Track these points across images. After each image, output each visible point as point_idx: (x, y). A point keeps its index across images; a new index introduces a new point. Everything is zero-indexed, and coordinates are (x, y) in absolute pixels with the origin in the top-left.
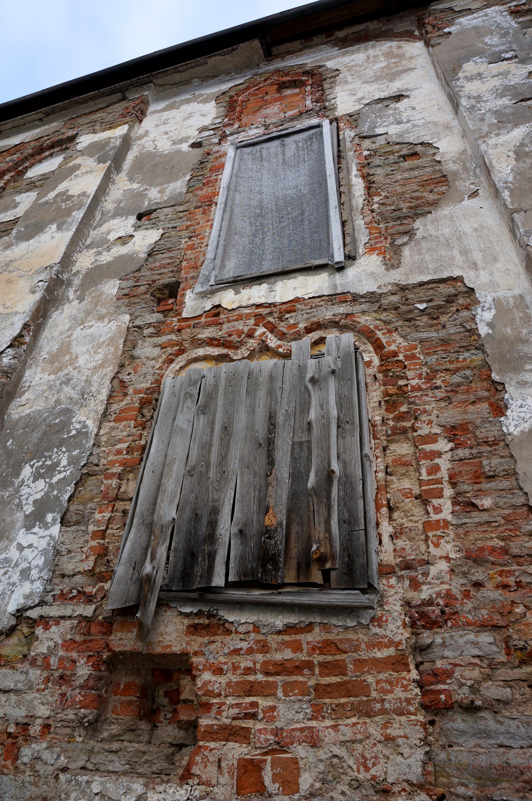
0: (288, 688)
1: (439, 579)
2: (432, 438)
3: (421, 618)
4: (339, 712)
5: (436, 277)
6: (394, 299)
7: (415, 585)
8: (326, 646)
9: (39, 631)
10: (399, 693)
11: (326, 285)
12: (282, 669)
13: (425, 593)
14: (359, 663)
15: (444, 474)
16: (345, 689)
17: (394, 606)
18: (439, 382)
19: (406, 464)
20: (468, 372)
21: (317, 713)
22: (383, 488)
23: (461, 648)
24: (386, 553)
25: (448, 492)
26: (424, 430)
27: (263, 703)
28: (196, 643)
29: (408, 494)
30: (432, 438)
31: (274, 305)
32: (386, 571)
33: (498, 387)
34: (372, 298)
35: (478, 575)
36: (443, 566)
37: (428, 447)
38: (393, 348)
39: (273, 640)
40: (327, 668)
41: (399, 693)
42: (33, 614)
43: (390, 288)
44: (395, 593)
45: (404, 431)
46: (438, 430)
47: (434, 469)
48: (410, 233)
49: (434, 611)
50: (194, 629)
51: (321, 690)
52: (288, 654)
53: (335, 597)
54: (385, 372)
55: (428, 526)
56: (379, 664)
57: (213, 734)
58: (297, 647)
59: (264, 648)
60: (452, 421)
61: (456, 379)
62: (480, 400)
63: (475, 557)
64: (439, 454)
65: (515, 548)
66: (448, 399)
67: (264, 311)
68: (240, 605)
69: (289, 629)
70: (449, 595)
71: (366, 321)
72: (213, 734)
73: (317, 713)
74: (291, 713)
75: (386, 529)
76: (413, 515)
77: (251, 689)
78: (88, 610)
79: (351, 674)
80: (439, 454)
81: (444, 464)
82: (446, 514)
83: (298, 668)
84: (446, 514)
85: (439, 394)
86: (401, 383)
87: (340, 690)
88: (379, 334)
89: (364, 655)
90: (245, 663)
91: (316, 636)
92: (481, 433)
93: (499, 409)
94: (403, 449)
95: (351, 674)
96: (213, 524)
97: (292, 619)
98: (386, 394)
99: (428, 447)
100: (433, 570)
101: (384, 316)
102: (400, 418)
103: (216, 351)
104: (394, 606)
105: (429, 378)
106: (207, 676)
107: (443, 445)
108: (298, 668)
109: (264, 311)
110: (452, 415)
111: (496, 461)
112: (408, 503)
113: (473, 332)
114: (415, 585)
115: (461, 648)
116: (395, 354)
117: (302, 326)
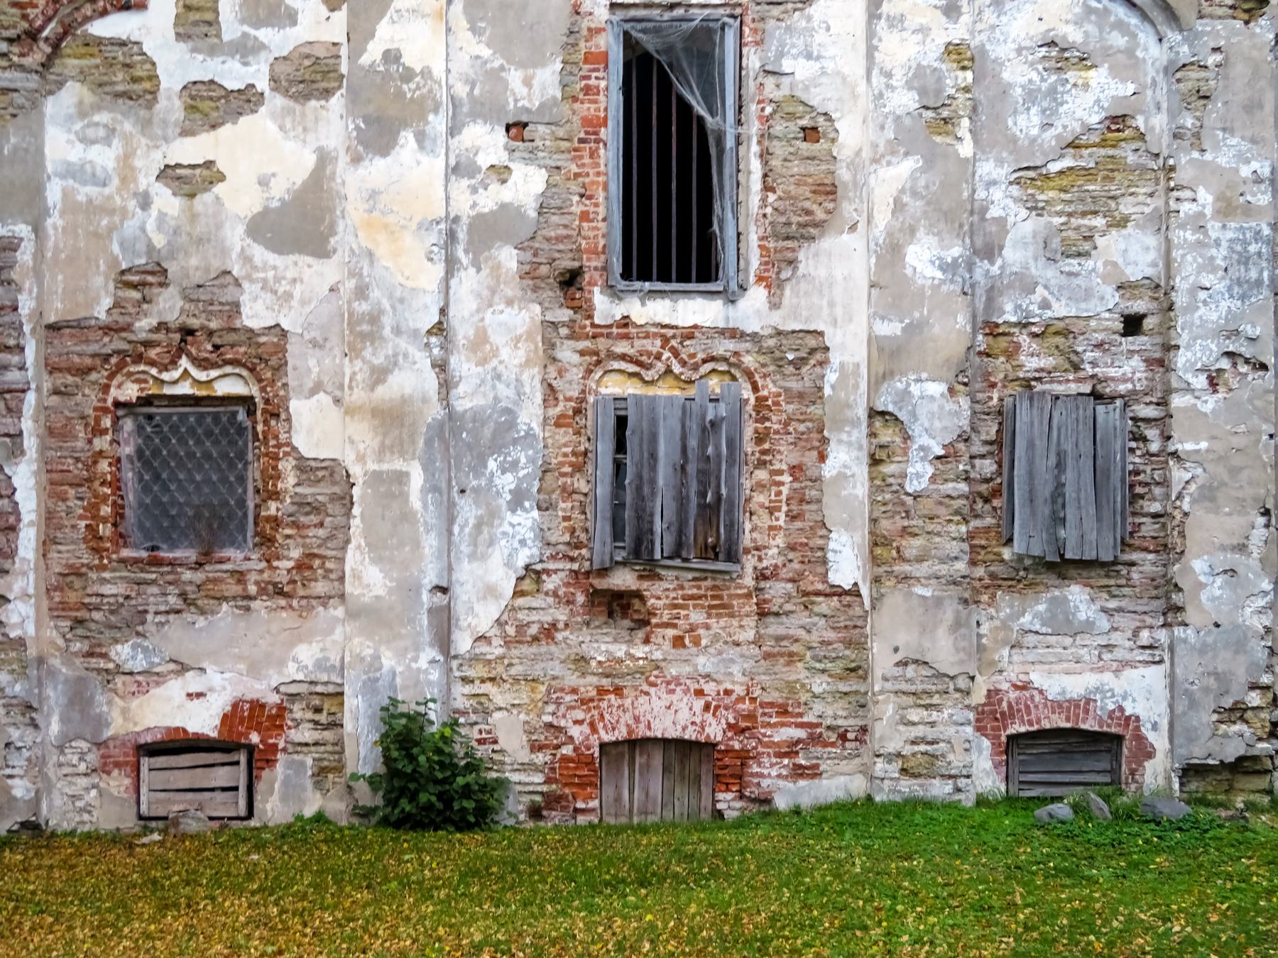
0: (695, 606)
1: (772, 557)
2: (780, 473)
3: (761, 576)
4: (719, 616)
5: (805, 328)
6: (771, 342)
7: (760, 559)
8: (714, 588)
9: (544, 577)
10: (747, 608)
11: (721, 316)
12: (692, 597)
13: (765, 563)
14: (730, 596)
15: (784, 497)
16: (723, 606)
17: (749, 570)
18: (791, 429)
19: (764, 486)
20: (810, 425)
21: (709, 616)
22: (748, 500)
23: (777, 590)
24: (746, 540)
25: (785, 508)
26: (777, 466)
27: (683, 612)
28: (645, 584)
29: (762, 506)
30: (780, 473)
31: (677, 327)
32: (747, 551)
33: (825, 441)
34: (754, 336)
35: (791, 555)
36: (775, 551)
37: (778, 478)
38: (765, 393)
39: (686, 584)
40: (713, 597)
41: (747, 608)
42: (539, 567)
43: (770, 331)
44: (750, 562)
45: (765, 463)
46: (785, 467)
47: (779, 493)
48: (792, 262)
49: (768, 572)
50: (641, 577)
51: (711, 607)
52: (695, 591)
53: (720, 566)
54: (758, 413)
55: (771, 528)
56: (739, 596)
57: (658, 625)
58: (699, 588)
59: (682, 588)
60: (795, 463)
61: (802, 428)
62: (812, 448)
63: (792, 548)
64: (782, 484)
65: (811, 544)
66: (795, 444)
67: (670, 332)
68: (668, 567)
69: (694, 579)
70: (776, 566)
71: (749, 361)
72: (658, 625)
73: (709, 616)
74: (697, 617)
75: (748, 526)
76: (764, 520)
77: (676, 606)
78: (575, 566)
79: (726, 600)
80: (782, 484)
81: (785, 490)
82: (781, 523)
83: (700, 597)
84: (781, 523)
85: (790, 439)
86: (768, 424)
87: (721, 608)
88: (757, 377)
89: (733, 591)
90: (672, 595)
91: (709, 583)
92: (809, 473)
93: (822, 458)
94: (762, 475)
95: (726, 600)
96: (651, 522)
97: (697, 575)
98: (756, 431)
99: (778, 478)
100: (770, 552)
101: (762, 359)
102: (764, 452)
103: (632, 368)
104: (749, 570)
105: (786, 424)
106: (653, 601)
107: (786, 478)
108: (700, 597)
109: (670, 332)
110: (794, 458)
111: (814, 493)
112: (761, 511)
113: (820, 389)
114: (760, 559)
115: (777, 590)
116: (766, 399)
117: (701, 356)
